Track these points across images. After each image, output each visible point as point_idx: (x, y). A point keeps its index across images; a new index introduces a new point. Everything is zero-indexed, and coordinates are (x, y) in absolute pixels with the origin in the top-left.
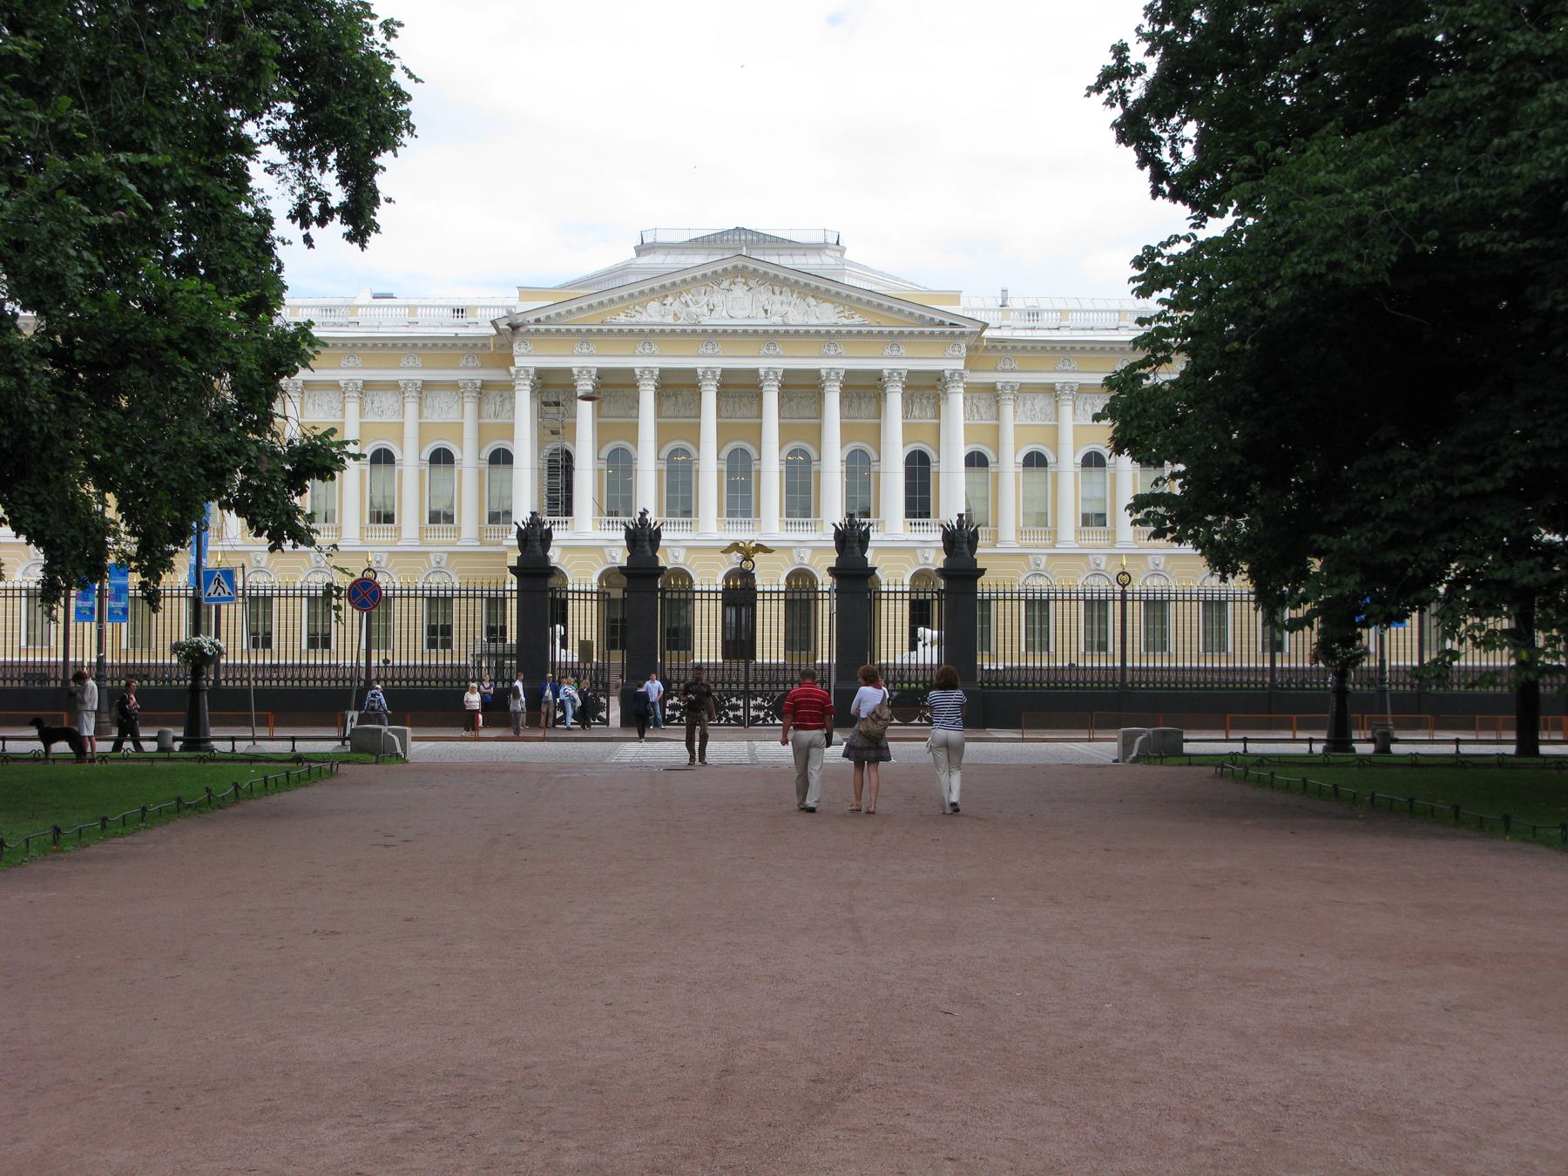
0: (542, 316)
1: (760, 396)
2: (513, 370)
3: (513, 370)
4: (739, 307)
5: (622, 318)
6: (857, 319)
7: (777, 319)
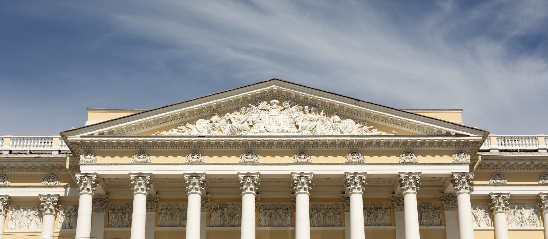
0: (105, 130)
1: (290, 207)
2: (78, 176)
3: (78, 176)
4: (275, 121)
5: (175, 132)
6: (375, 132)
7: (306, 133)
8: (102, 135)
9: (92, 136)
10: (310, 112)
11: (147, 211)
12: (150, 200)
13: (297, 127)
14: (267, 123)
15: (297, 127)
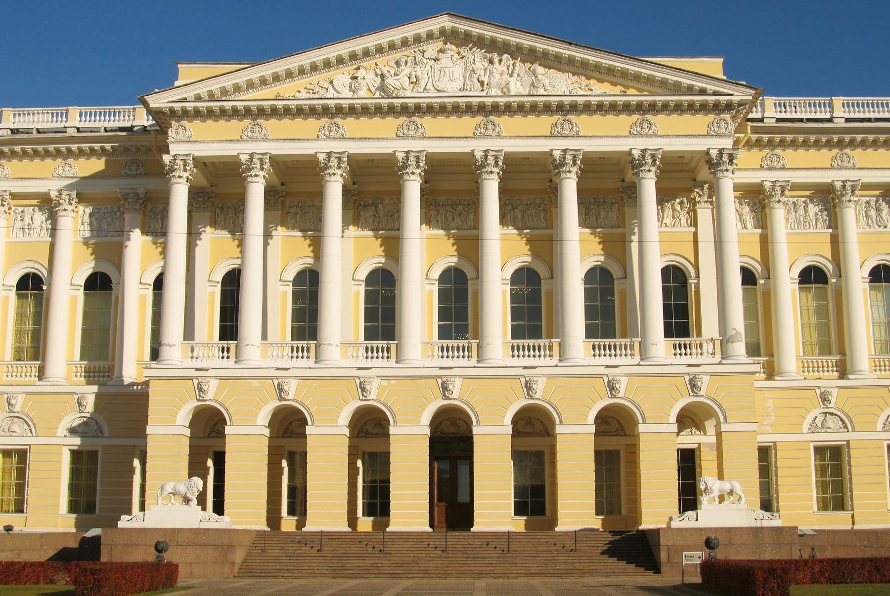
2: (166, 159)
3: (166, 159)
5: (304, 94)
8: (198, 99)
9: (185, 100)
10: (500, 61)
11: (265, 211)
12: (270, 193)
13: (482, 83)
14: (437, 78)
15: (482, 83)
